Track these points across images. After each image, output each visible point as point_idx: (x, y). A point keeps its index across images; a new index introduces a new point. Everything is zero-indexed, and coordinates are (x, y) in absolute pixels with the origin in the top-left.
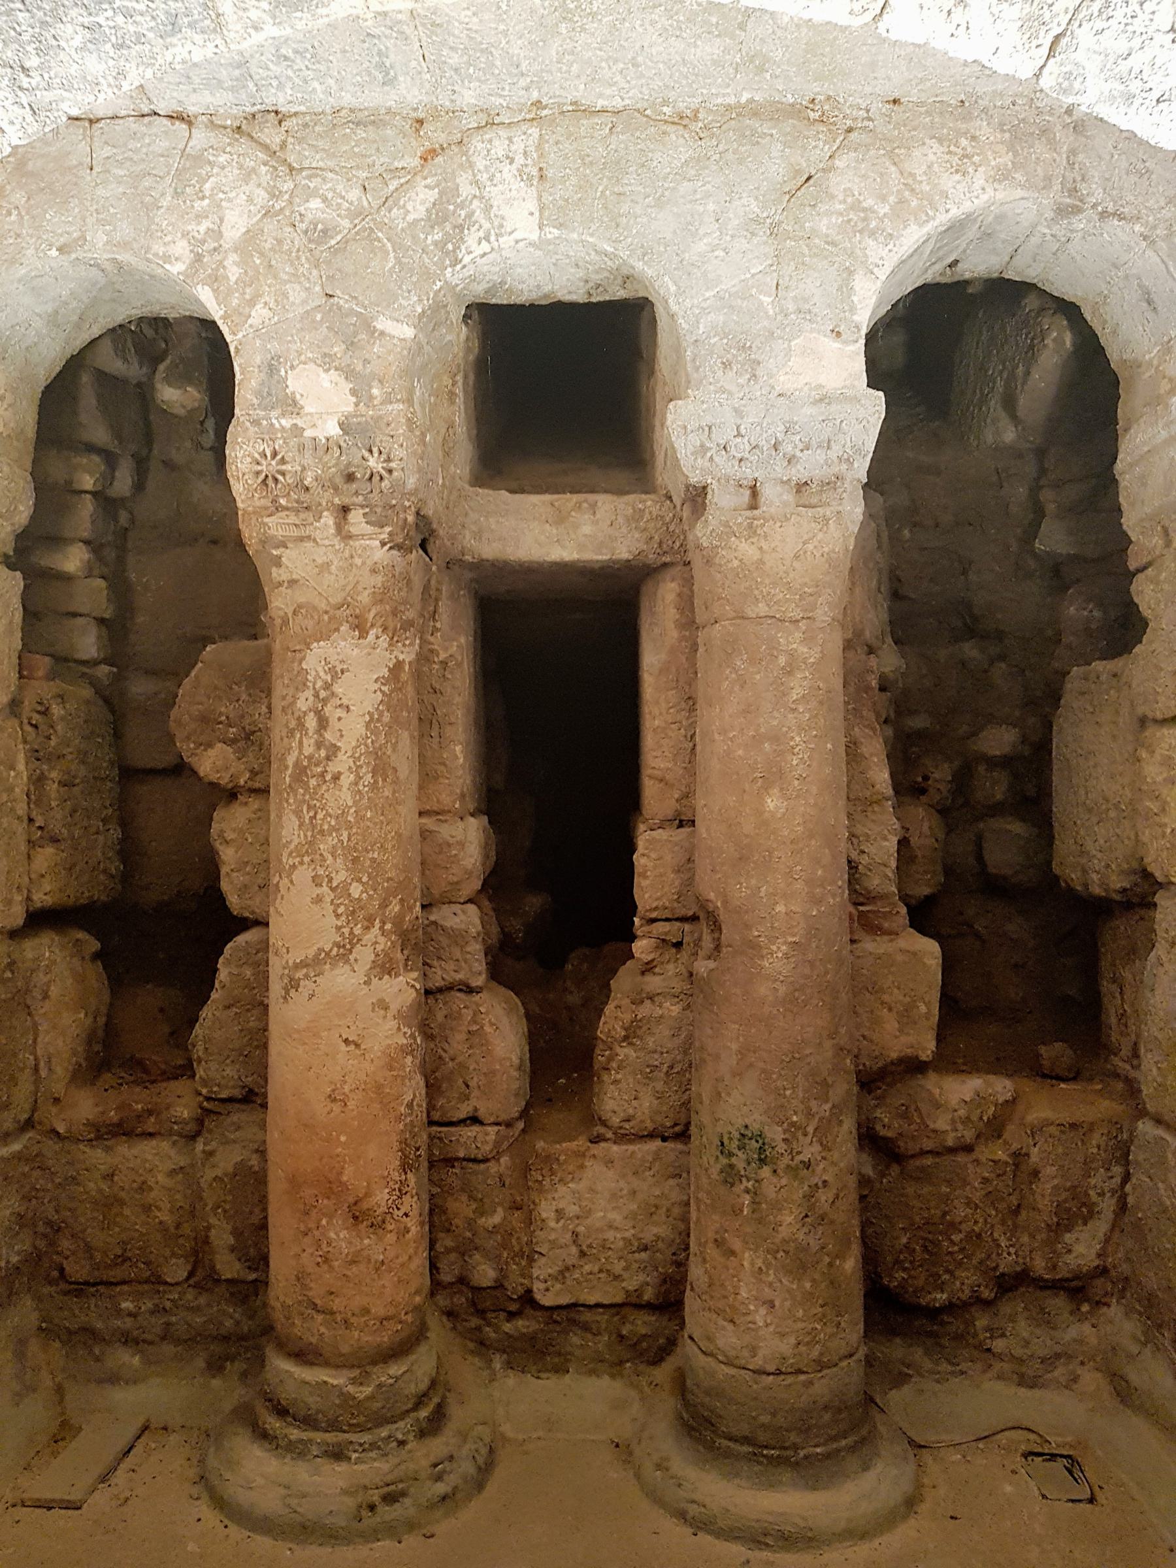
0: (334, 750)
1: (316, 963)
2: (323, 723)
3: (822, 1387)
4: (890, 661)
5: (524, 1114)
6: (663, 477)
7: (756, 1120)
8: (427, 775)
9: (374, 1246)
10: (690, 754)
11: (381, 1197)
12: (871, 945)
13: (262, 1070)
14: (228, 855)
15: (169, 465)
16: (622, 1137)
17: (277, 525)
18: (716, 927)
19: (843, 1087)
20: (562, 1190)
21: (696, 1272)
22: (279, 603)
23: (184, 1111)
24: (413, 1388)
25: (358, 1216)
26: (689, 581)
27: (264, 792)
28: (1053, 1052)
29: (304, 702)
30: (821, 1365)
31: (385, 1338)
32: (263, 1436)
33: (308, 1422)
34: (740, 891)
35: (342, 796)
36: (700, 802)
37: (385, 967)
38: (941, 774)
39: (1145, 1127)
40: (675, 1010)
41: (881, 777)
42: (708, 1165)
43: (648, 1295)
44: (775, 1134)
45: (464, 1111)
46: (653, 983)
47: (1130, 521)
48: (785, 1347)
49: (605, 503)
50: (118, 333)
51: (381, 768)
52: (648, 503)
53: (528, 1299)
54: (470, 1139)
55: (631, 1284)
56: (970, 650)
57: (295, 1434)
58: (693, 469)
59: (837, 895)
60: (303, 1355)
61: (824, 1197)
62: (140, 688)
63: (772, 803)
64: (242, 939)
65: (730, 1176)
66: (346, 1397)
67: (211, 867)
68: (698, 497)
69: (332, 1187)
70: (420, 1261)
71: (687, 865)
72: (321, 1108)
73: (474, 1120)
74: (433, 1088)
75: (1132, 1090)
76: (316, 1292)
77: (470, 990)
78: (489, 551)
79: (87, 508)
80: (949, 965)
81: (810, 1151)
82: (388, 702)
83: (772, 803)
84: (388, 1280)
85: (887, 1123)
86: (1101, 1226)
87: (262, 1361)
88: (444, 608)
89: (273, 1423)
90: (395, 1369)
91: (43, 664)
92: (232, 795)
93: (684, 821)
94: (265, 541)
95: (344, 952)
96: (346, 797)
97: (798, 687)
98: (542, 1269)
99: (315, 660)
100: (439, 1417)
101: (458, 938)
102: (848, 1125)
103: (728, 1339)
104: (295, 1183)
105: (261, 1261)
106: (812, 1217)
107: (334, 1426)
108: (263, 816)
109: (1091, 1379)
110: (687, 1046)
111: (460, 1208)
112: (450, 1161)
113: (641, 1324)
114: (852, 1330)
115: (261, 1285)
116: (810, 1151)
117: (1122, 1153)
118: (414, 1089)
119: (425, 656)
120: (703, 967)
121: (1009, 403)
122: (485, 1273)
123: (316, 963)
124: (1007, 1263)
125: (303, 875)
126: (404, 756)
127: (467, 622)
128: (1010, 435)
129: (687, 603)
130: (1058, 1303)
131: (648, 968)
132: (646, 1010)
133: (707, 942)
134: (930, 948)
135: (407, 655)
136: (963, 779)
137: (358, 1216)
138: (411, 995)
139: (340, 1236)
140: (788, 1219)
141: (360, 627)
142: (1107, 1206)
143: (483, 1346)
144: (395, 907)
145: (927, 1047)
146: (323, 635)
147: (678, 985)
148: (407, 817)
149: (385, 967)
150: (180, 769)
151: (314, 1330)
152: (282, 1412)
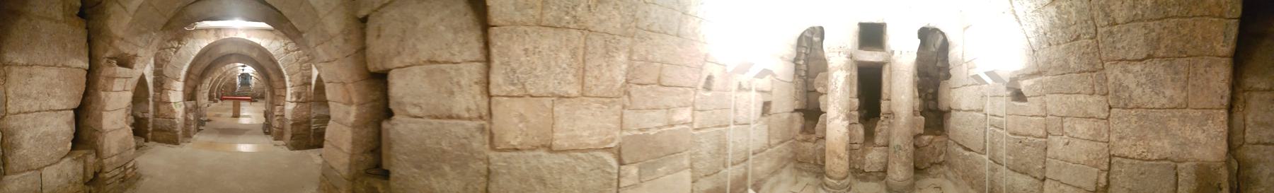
0: (837, 88)
1: (834, 119)
2: (836, 84)
3: (908, 182)
4: (917, 79)
5: (864, 142)
6: (887, 49)
7: (899, 144)
8: (851, 92)
9: (841, 162)
10: (890, 90)
11: (842, 155)
12: (916, 118)
13: (825, 134)
14: (821, 103)
15: (814, 49)
16: (879, 146)
17: (830, 55)
18: (894, 115)
19: (912, 138)
20: (869, 154)
21: (890, 167)
22: (830, 66)
23: (814, 139)
24: (847, 183)
25: (839, 157)
26: (890, 65)
27: (826, 94)
28: (938, 132)
29: (833, 80)
30: (908, 179)
31: (842, 176)
32: (824, 189)
33: (830, 187)
34: (898, 110)
35: (838, 94)
36: (892, 96)
37: (844, 120)
38: (923, 95)
39: (950, 141)
40: (887, 127)
41: (917, 94)
42: (891, 150)
43: (882, 170)
44: (902, 145)
45: (854, 142)
46: (883, 123)
47: (950, 62)
48: (903, 177)
49: (878, 53)
50: (808, 30)
51: (844, 90)
52: (885, 53)
53: (864, 171)
54: (855, 146)
55: (879, 168)
56: (928, 78)
57: (829, 189)
58: (892, 48)
59: (912, 111)
60: (830, 177)
61: (909, 155)
62: (810, 80)
63: (903, 97)
64: (823, 115)
65: (895, 152)
66: (836, 185)
67: (818, 104)
68: (893, 52)
69: (835, 152)
70: (848, 164)
71: (889, 106)
72: (834, 140)
73: (856, 143)
74: (850, 138)
75: (948, 136)
76: (832, 168)
77: (856, 124)
78: (861, 59)
79: (803, 55)
80: (925, 120)
81: (907, 147)
82: (846, 81)
83: (903, 97)
84: (843, 168)
85: (917, 143)
86: (943, 155)
87: (824, 177)
88: (854, 68)
89: (825, 187)
90: (844, 181)
91: (797, 76)
92: (822, 94)
93: (889, 100)
94: (828, 57)
95: (838, 117)
96: (839, 94)
97: (907, 80)
98: (866, 166)
99: (835, 75)
100: (850, 188)
101: (855, 116)
102: (912, 143)
103: (895, 176)
104: (829, 151)
105: (824, 162)
106: (907, 157)
107: (834, 189)
108: (827, 97)
109: (942, 176)
110: (889, 133)
111: (854, 157)
112: (852, 149)
113: (880, 174)
114: (912, 174)
115: (824, 166)
116: (907, 147)
117: (946, 145)
118: (848, 138)
119: (851, 75)
120: (892, 121)
121: (934, 45)
122: (857, 167)
123: (834, 119)
124: (932, 161)
125: (832, 106)
126: (848, 90)
127: (857, 70)
128: (934, 50)
129: (890, 68)
130: (938, 166)
131: (883, 121)
132: (883, 127)
133: (892, 117)
134: (923, 118)
135: (848, 74)
136: (926, 95)
137: (839, 157)
138: (847, 124)
139: (836, 160)
140: (904, 158)
141: (841, 69)
142: (944, 152)
143: (857, 178)
144: (845, 111)
145: (922, 132)
146: (835, 71)
147: (887, 123)
148: (848, 98)
149: (844, 120)
150: (815, 91)
151: (832, 174)
152: (827, 185)
